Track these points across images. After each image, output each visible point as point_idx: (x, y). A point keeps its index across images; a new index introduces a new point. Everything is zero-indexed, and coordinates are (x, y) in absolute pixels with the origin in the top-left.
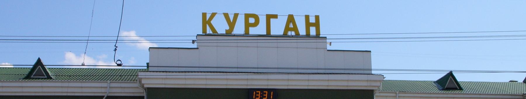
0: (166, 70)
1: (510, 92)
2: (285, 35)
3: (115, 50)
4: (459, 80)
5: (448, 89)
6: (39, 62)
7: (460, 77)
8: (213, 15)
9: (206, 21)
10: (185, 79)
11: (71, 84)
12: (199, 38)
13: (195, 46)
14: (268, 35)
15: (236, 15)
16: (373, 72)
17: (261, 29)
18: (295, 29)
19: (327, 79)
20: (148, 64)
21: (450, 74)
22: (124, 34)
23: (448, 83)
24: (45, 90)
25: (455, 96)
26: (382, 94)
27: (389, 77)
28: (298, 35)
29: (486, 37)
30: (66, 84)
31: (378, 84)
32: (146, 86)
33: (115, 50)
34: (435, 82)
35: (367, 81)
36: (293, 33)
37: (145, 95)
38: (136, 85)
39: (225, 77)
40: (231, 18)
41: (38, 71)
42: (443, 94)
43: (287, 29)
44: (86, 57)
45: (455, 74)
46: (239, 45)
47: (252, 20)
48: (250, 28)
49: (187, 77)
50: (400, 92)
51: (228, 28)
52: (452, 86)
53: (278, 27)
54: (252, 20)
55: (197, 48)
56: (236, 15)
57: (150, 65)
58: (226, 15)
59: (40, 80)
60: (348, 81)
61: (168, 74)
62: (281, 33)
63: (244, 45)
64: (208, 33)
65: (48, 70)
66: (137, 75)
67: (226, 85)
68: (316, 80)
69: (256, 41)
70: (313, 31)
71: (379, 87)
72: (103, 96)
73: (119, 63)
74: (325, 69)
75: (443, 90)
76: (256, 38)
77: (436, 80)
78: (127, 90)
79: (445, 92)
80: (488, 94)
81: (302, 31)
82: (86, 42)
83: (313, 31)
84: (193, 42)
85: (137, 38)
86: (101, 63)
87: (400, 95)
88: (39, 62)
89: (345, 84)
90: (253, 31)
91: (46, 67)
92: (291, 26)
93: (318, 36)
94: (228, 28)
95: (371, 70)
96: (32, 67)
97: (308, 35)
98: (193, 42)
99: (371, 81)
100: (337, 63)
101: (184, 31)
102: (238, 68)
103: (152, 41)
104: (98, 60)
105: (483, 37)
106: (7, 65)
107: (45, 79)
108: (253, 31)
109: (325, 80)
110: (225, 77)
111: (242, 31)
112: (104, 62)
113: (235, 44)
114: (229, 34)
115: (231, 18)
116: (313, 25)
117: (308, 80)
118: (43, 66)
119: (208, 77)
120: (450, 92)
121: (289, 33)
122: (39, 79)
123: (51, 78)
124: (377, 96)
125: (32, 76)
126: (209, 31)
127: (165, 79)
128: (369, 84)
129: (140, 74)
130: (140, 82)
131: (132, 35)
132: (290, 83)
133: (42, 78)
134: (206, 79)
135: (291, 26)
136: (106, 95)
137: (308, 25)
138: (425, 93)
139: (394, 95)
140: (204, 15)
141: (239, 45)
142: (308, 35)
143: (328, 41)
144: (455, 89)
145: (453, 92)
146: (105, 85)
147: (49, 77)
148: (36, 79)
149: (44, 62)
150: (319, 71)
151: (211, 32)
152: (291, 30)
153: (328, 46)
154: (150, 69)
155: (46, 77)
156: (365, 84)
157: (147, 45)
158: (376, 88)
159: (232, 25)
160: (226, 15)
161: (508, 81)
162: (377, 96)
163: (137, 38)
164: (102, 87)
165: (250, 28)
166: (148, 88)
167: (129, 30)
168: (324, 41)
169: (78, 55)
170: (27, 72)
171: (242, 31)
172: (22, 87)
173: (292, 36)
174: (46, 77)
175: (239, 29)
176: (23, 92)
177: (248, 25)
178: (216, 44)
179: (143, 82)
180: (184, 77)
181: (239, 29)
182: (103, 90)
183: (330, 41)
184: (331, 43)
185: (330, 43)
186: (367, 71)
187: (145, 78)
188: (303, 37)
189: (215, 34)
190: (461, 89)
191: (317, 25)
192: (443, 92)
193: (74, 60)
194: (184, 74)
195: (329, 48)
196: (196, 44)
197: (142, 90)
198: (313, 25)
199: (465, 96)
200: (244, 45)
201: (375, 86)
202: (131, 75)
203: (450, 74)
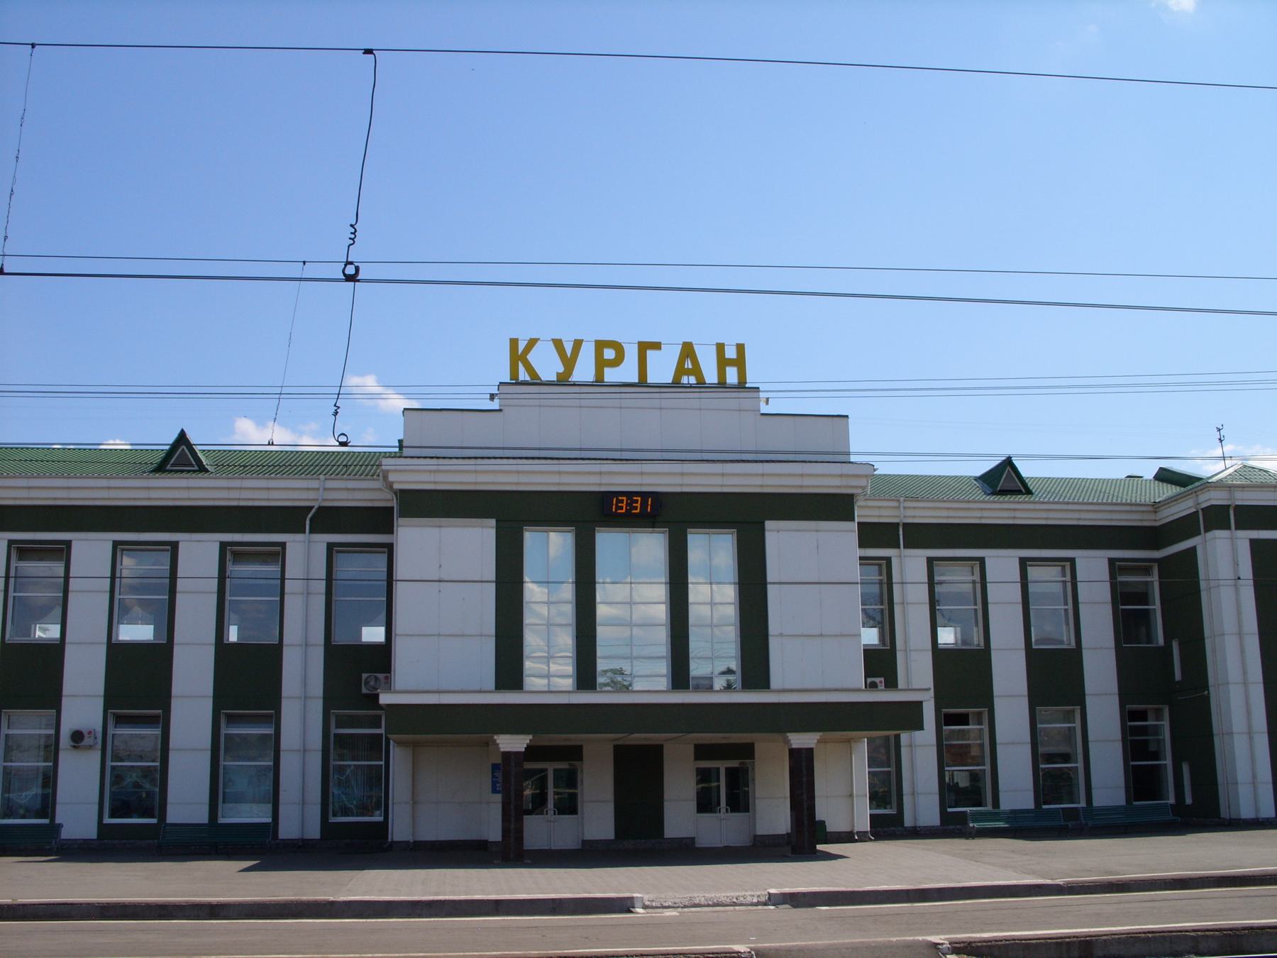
0: (437, 454)
1: (1127, 498)
2: (676, 384)
3: (336, 413)
4: (1024, 474)
5: (1003, 492)
6: (182, 438)
7: (1026, 469)
8: (532, 343)
9: (518, 355)
10: (476, 472)
11: (272, 484)
12: (504, 389)
13: (495, 405)
14: (642, 383)
15: (578, 344)
16: (853, 458)
17: (627, 372)
18: (697, 371)
19: (760, 472)
20: (400, 441)
21: (1008, 463)
22: (352, 381)
23: (1004, 480)
24: (113, 494)
25: (1018, 506)
26: (870, 503)
27: (884, 468)
28: (701, 384)
29: (1069, 387)
30: (237, 483)
31: (863, 482)
32: (396, 486)
33: (336, 413)
34: (977, 479)
35: (841, 476)
36: (693, 380)
37: (394, 504)
38: (377, 484)
39: (555, 468)
40: (569, 348)
41: (180, 457)
42: (1025, 502)
43: (680, 371)
44: (277, 427)
45: (1017, 463)
46: (584, 403)
47: (609, 354)
48: (607, 370)
49: (479, 468)
50: (907, 499)
51: (561, 369)
52: (1010, 486)
53: (662, 368)
54: (609, 354)
55: (500, 410)
56: (578, 344)
57: (405, 444)
58: (558, 344)
59: (184, 475)
60: (802, 475)
61: (441, 461)
62: (669, 379)
63: (594, 403)
64: (521, 379)
65: (200, 455)
66: (380, 465)
67: (558, 484)
68: (818, 475)
69: (618, 396)
70: (732, 376)
71: (864, 488)
72: (312, 508)
73: (343, 439)
74: (757, 452)
75: (993, 493)
76: (617, 390)
77: (979, 474)
78: (358, 495)
79: (996, 498)
80: (1083, 503)
81: (711, 377)
82: (277, 398)
83: (732, 376)
84: (492, 397)
85: (379, 390)
86: (306, 440)
87: (907, 504)
88: (182, 438)
89: (798, 482)
90: (611, 375)
91: (197, 448)
92: (688, 365)
93: (741, 385)
94: (561, 369)
95: (848, 454)
96: (167, 447)
97: (722, 384)
98: (492, 397)
99: (848, 476)
100: (780, 439)
101: (474, 376)
102: (581, 450)
103: (408, 396)
104: (301, 434)
105: (1069, 387)
106: (117, 443)
107: (194, 471)
108: (611, 375)
109: (757, 475)
110: (555, 468)
111: (590, 377)
112: (312, 437)
113: (577, 403)
114: (563, 381)
115: (569, 348)
116: (731, 362)
117: (723, 475)
118: (190, 446)
119: (521, 468)
120: (1007, 498)
121: (685, 380)
122: (182, 471)
123: (207, 471)
124: (860, 507)
125: (168, 467)
126: (523, 375)
127: (435, 471)
128: (844, 482)
129: (385, 461)
130: (385, 478)
131: (370, 383)
132: (687, 480)
133: (189, 471)
134: (518, 472)
135: (688, 365)
136: (316, 505)
137: (723, 363)
138: (958, 501)
139: (895, 504)
140: (514, 343)
141: (584, 403)
142: (722, 384)
143: (762, 395)
144: (1019, 492)
145: (1013, 498)
146: (315, 484)
147: (202, 469)
148: (177, 471)
149: (193, 438)
150: (745, 457)
151: (528, 378)
152: (688, 372)
153: (762, 404)
154: (406, 452)
155: (196, 468)
156: (837, 482)
157: (401, 403)
158: (860, 491)
159: (570, 363)
160: (558, 344)
161: (1123, 476)
162: (860, 507)
163: (379, 390)
164: (308, 489)
165: (607, 370)
166: (402, 491)
167: (362, 374)
168: (755, 395)
169: (260, 423)
170: (158, 459)
171: (590, 377)
172: (148, 488)
173: (691, 386)
174: (196, 468)
175: (584, 371)
176: (150, 499)
177: (601, 364)
178: (537, 402)
179: (391, 478)
180: (472, 468)
181: (584, 371)
182: (312, 495)
183: (767, 395)
184: (768, 399)
185: (767, 402)
186: (841, 457)
187: (396, 471)
188: (711, 386)
189: (536, 381)
190: (1029, 492)
191: (740, 362)
192: (992, 498)
193: (253, 433)
194: (473, 461)
195: (764, 409)
196: (497, 401)
197: (389, 495)
198: (731, 362)
199: (1038, 506)
200: (594, 403)
201: (856, 487)
202: (368, 464)
203: (1008, 463)
